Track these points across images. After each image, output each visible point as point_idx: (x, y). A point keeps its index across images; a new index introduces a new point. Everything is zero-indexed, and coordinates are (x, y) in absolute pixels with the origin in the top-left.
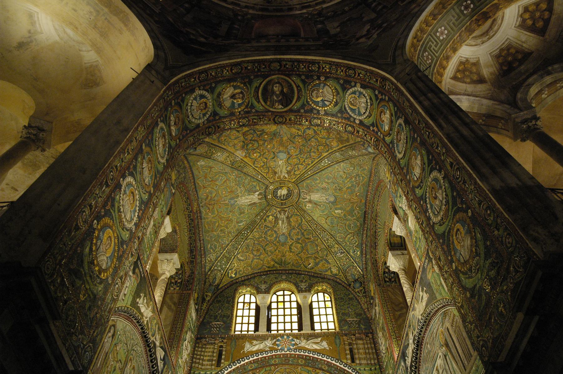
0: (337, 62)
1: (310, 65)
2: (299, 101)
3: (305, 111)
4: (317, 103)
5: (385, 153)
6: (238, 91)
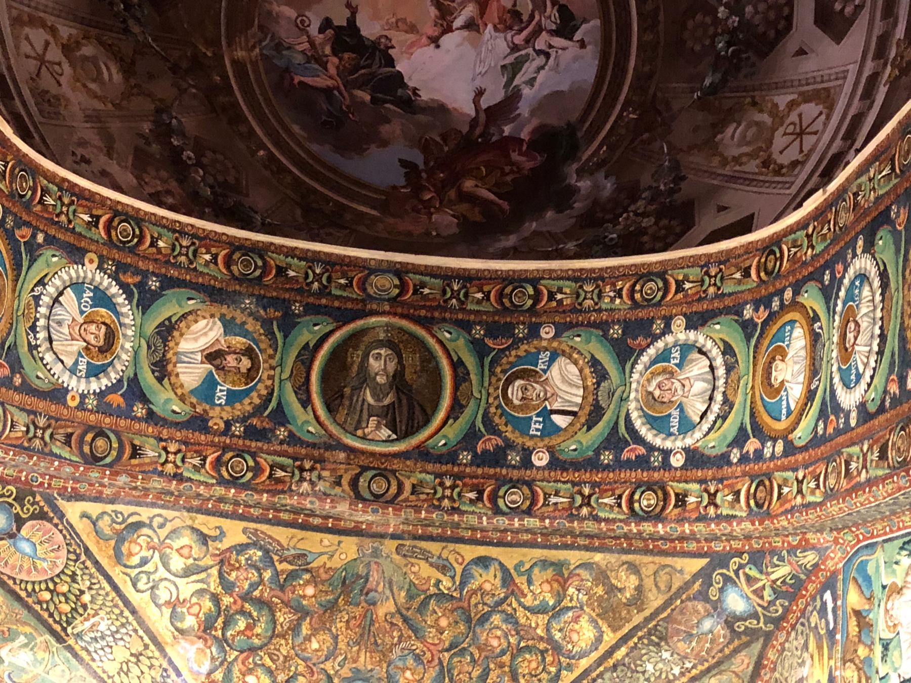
0: (601, 269)
1: (508, 290)
2: (456, 419)
3: (475, 455)
4: (523, 426)
5: (800, 491)
6: (239, 341)
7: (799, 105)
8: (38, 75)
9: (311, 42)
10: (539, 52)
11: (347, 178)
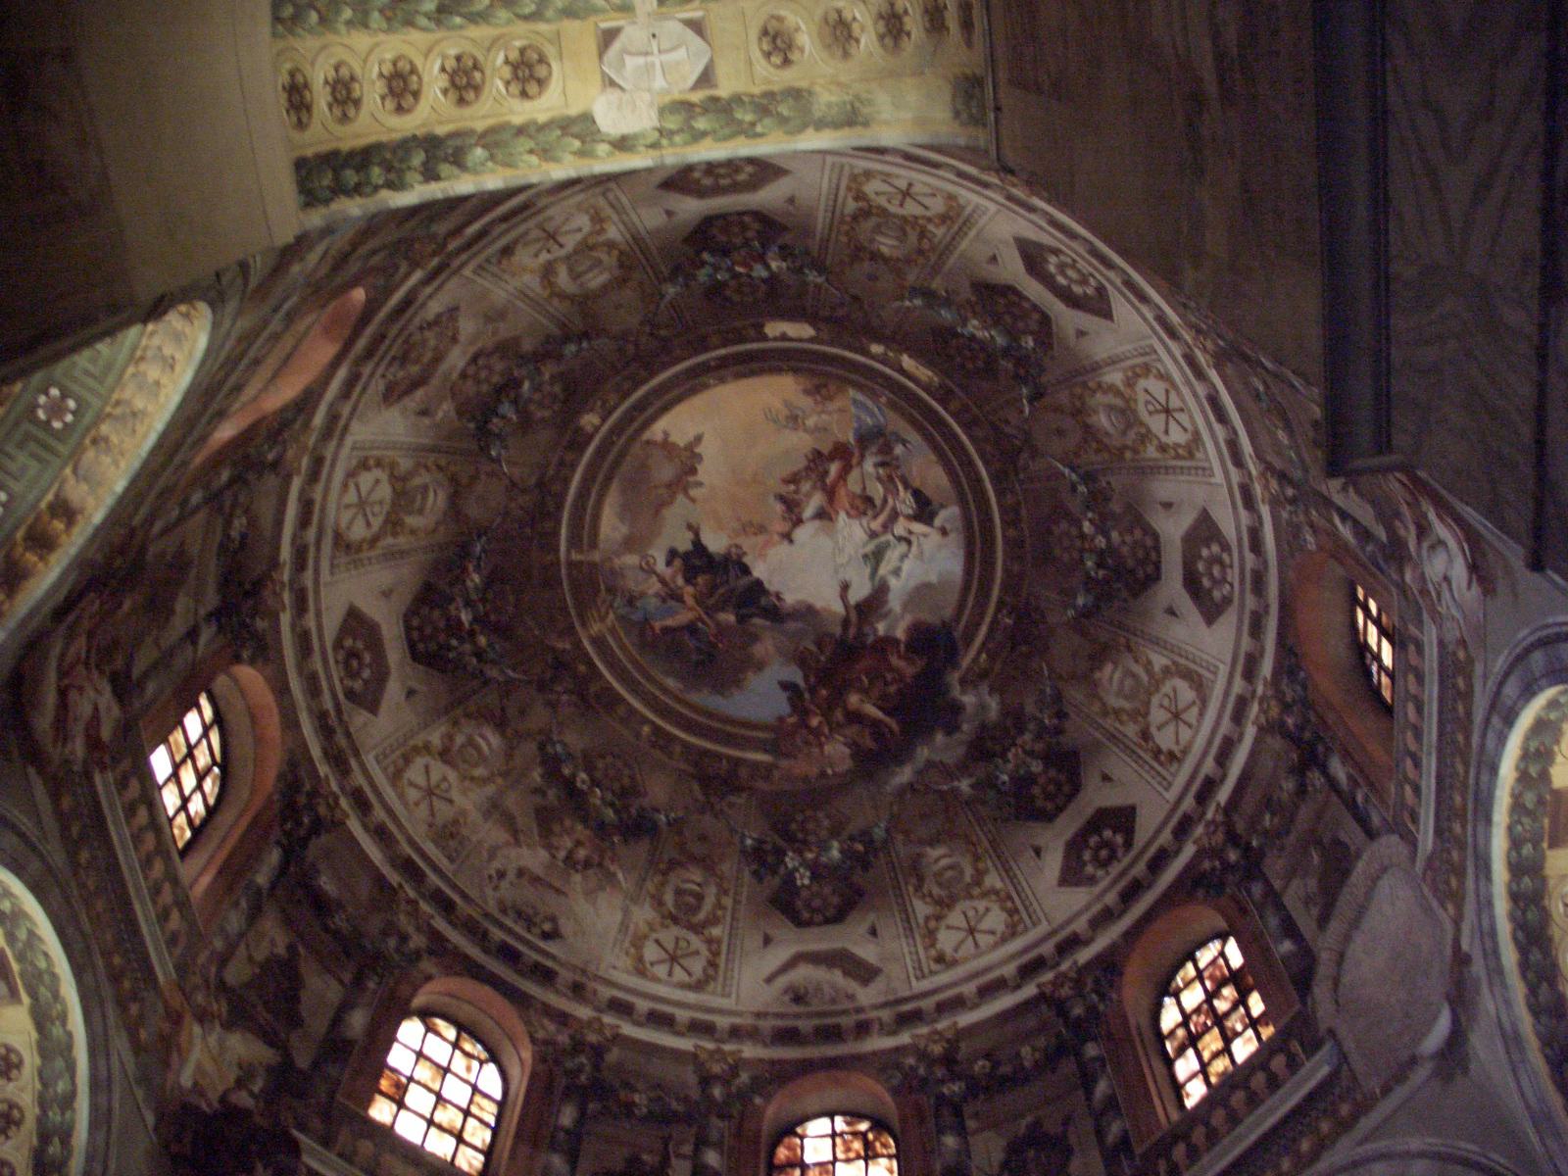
7: (1172, 675)
8: (433, 814)
9: (662, 581)
10: (900, 539)
11: (733, 722)
